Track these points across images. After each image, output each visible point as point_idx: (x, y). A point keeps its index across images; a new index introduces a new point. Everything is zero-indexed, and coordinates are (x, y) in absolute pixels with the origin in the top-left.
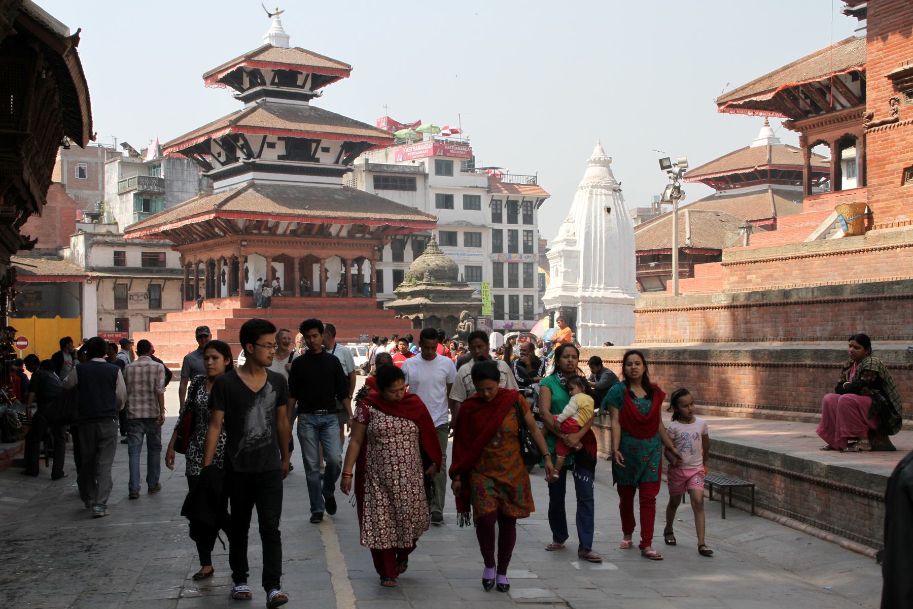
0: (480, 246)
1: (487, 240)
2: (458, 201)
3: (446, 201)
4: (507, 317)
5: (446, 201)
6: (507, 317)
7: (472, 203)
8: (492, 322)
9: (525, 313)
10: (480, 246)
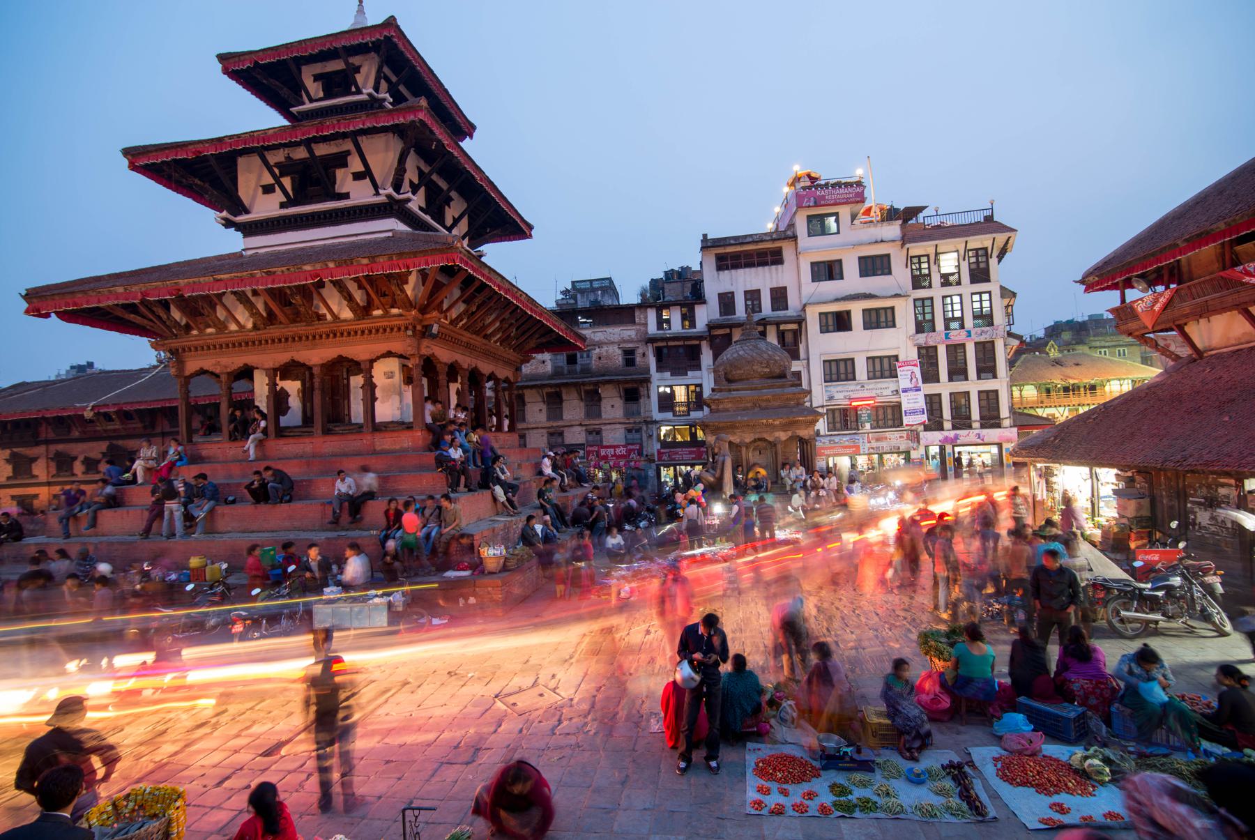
0: (894, 326)
1: (905, 314)
2: (851, 268)
3: (828, 270)
4: (948, 425)
5: (828, 270)
6: (948, 425)
7: (874, 266)
8: (918, 435)
9: (982, 418)
10: (894, 326)
